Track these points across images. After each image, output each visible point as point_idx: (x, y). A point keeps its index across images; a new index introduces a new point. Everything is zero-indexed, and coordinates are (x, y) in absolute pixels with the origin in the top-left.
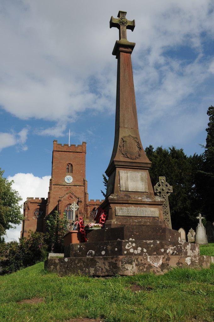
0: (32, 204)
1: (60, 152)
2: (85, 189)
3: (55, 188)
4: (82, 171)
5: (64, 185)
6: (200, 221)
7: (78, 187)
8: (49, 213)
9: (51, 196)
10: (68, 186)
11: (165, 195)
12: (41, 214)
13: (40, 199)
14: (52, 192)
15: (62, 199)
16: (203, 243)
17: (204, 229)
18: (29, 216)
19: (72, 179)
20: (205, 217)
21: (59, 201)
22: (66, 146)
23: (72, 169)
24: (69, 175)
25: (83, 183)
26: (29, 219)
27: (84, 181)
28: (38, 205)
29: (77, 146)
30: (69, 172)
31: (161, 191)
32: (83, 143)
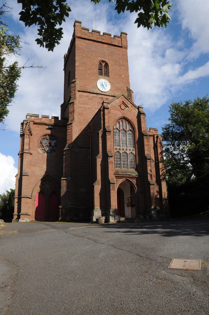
0: (36, 126)
1: (86, 41)
3: (81, 97)
4: (123, 76)
8: (73, 140)
12: (53, 144)
13: (50, 118)
18: (31, 146)
22: (96, 34)
26: (31, 152)
27: (129, 91)
28: (47, 129)
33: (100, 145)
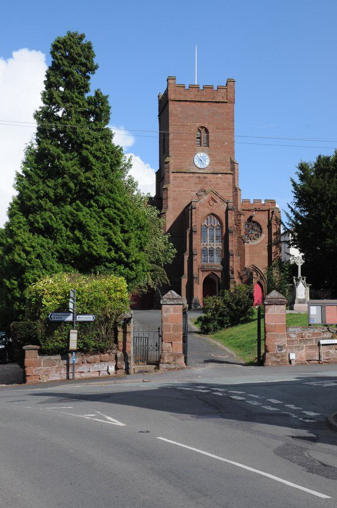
2: (234, 179)
4: (226, 143)
7: (220, 175)
10: (200, 175)
19: (208, 160)
22: (194, 90)
24: (202, 152)
25: (229, 167)
27: (233, 163)
29: (215, 88)
30: (201, 145)
33: (188, 243)
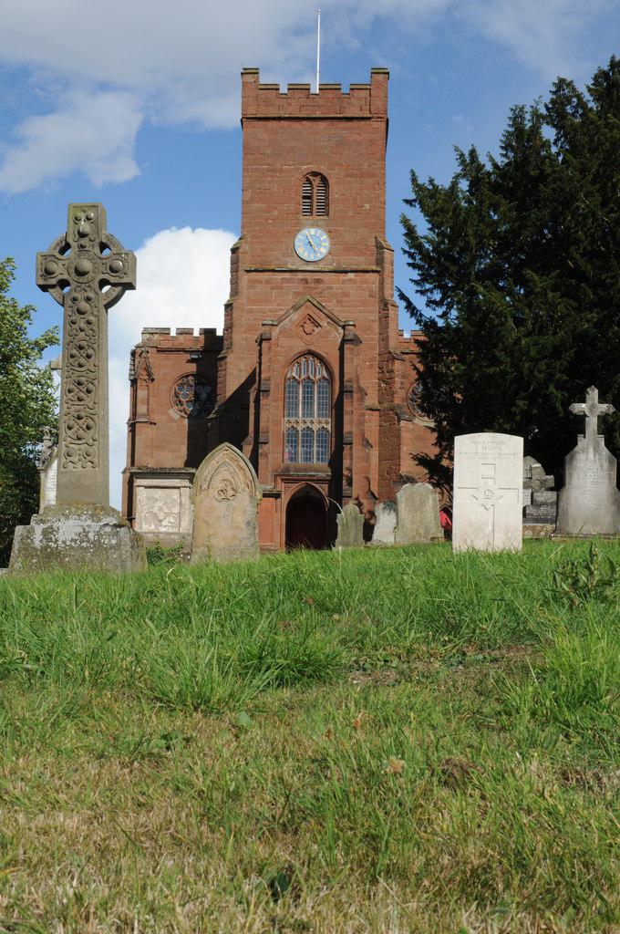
0: (163, 355)
1: (271, 124)
2: (382, 283)
3: (252, 283)
4: (367, 206)
5: (291, 271)
6: (592, 424)
7: (351, 275)
8: (229, 394)
9: (236, 322)
10: (310, 275)
11: (88, 299)
12: (204, 396)
13: (196, 333)
14: (242, 301)
15: (275, 332)
16: (591, 529)
17: (610, 462)
18: (152, 403)
19: (327, 244)
20: (613, 403)
21: (261, 341)
22: (298, 94)
23: (327, 198)
24: (312, 226)
25: (373, 258)
26: (155, 418)
28: (189, 361)
29: (345, 89)
30: (311, 212)
31: (72, 278)
32: (376, 72)
33: (252, 417)
